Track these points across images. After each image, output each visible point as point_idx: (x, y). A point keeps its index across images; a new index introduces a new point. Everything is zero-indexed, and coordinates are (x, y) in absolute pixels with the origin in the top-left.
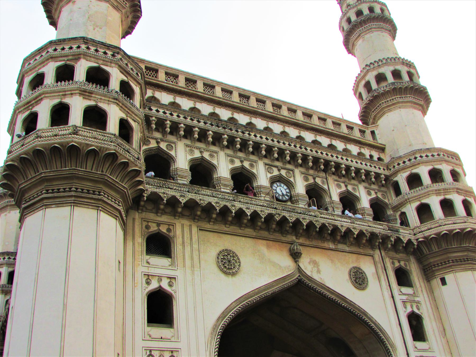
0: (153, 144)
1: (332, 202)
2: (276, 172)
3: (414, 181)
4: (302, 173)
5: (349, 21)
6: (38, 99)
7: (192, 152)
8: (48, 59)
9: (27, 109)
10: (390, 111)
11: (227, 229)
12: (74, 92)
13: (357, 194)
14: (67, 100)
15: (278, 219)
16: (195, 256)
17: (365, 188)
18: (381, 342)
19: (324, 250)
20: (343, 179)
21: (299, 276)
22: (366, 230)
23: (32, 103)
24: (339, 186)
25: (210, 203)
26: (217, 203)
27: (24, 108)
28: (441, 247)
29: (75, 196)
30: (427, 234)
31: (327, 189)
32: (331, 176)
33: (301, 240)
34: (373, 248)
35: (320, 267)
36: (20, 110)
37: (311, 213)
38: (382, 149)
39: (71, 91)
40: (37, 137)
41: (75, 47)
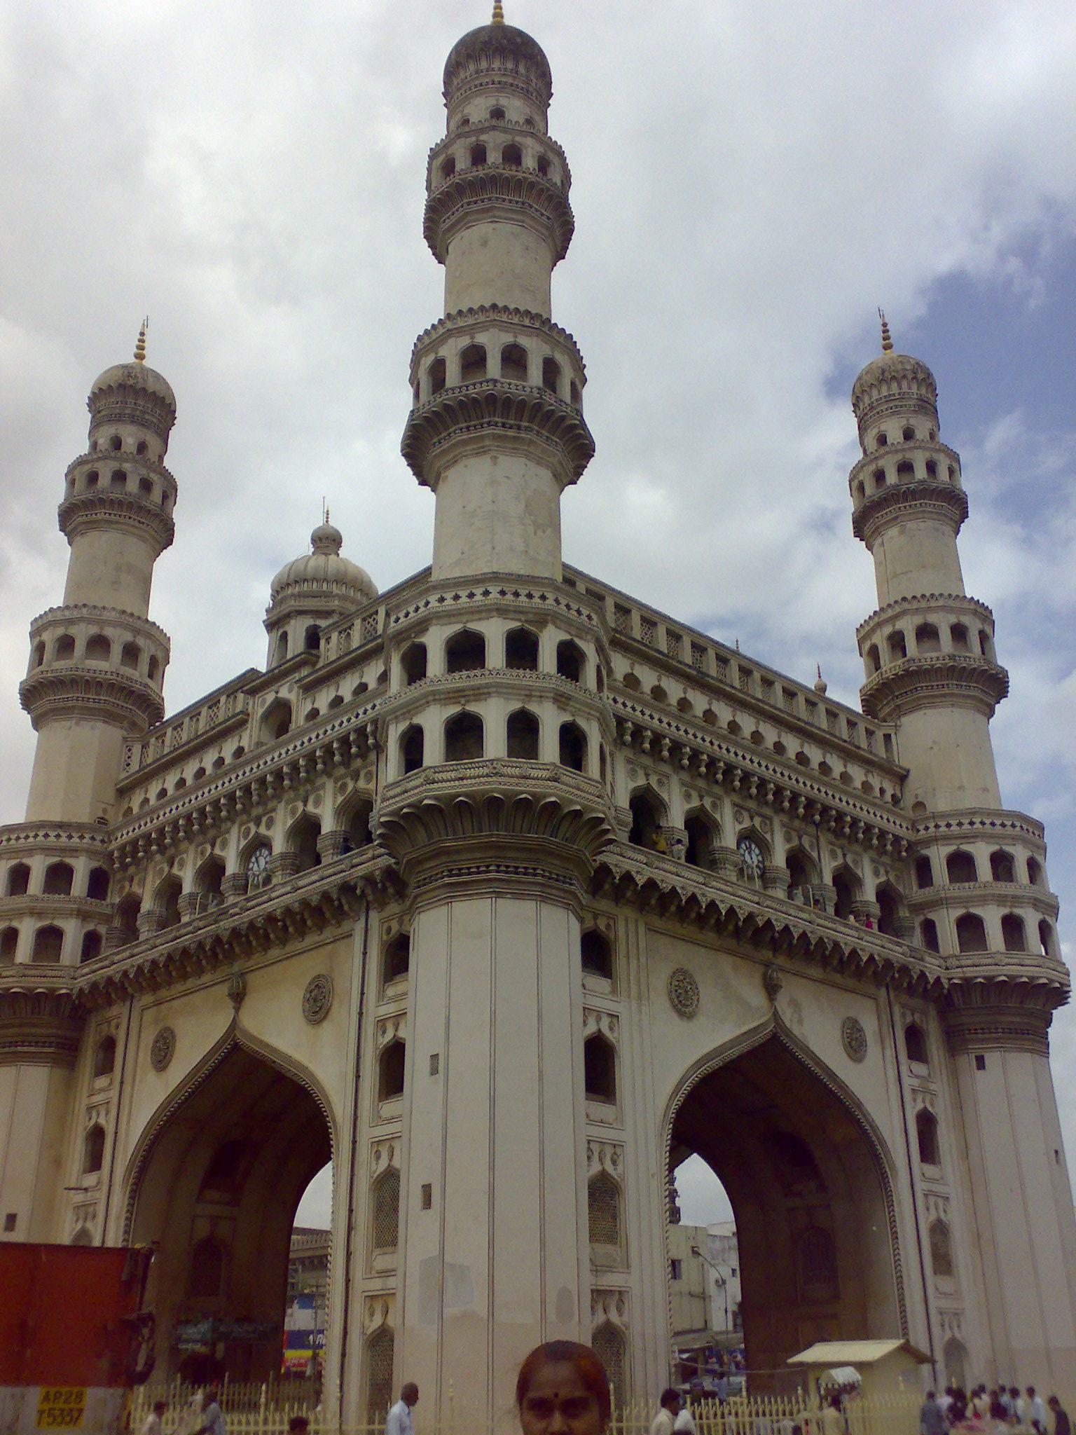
1: (822, 886)
3: (961, 865)
5: (880, 476)
7: (632, 774)
8: (490, 611)
10: (932, 706)
14: (534, 708)
17: (873, 860)
18: (876, 1157)
24: (833, 855)
25: (674, 890)
26: (683, 888)
30: (970, 972)
34: (878, 986)
37: (805, 916)
38: (902, 778)
40: (495, 774)
41: (537, 594)
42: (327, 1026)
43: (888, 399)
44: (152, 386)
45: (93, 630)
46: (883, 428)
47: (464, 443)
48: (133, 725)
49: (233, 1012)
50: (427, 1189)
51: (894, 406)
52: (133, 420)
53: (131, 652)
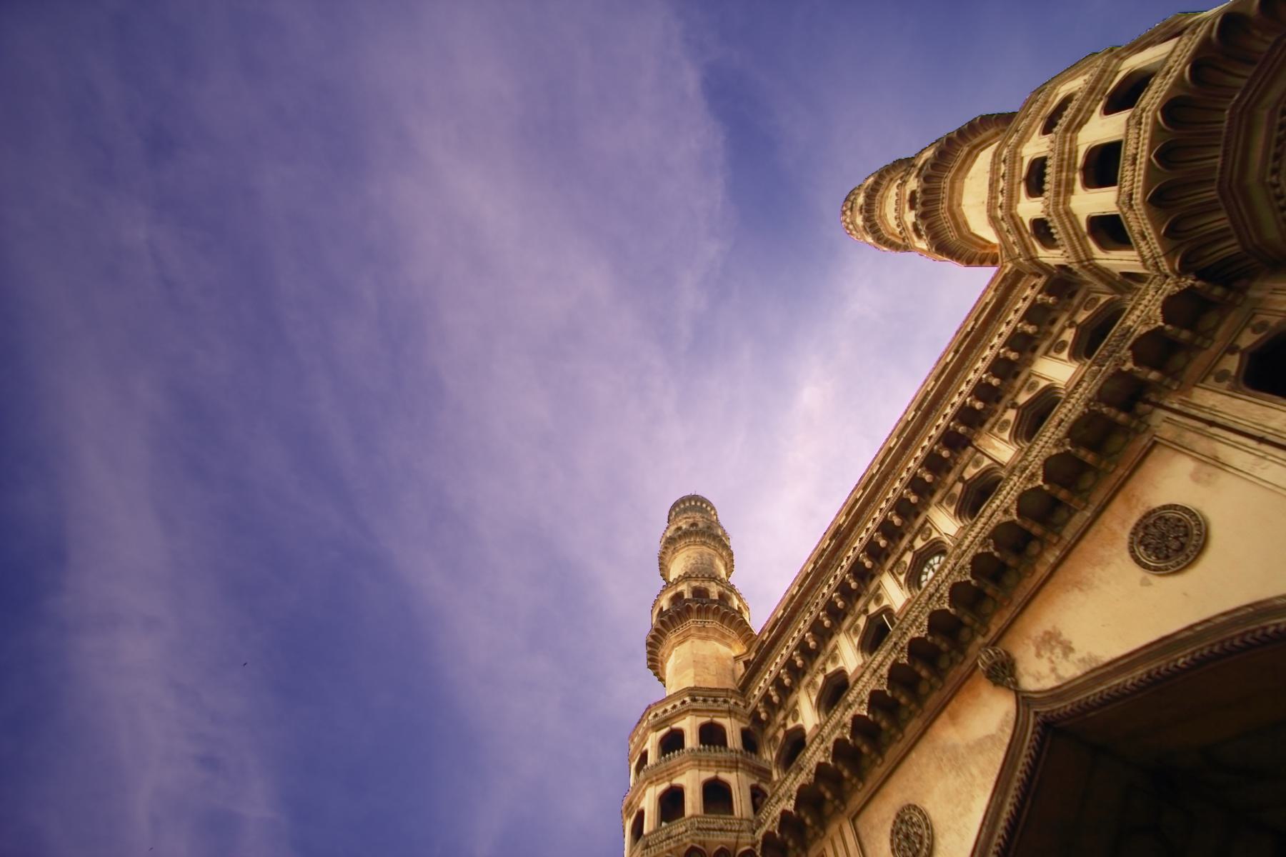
0: (781, 734)
2: (908, 558)
4: (940, 502)
10: (966, 223)
11: (883, 769)
13: (1043, 383)
15: (905, 661)
17: (1046, 353)
19: (1048, 587)
20: (1000, 408)
21: (1036, 713)
22: (1056, 446)
25: (819, 765)
28: (1216, 201)
31: (990, 462)
32: (980, 434)
33: (994, 630)
35: (1066, 636)
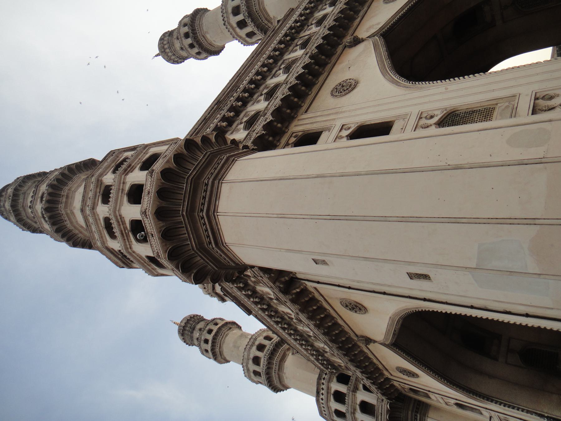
5: (192, 46)
6: (120, 220)
7: (238, 130)
9: (128, 236)
11: (312, 94)
12: (122, 180)
16: (329, 113)
23: (123, 229)
25: (282, 100)
27: (126, 240)
29: (214, 179)
36: (128, 246)
39: (120, 183)
40: (146, 213)
42: (366, 304)
43: (169, 48)
44: (183, 324)
45: (251, 362)
46: (179, 49)
47: (71, 223)
48: (288, 349)
49: (376, 344)
50: (412, 276)
51: (171, 45)
52: (192, 333)
53: (261, 348)
